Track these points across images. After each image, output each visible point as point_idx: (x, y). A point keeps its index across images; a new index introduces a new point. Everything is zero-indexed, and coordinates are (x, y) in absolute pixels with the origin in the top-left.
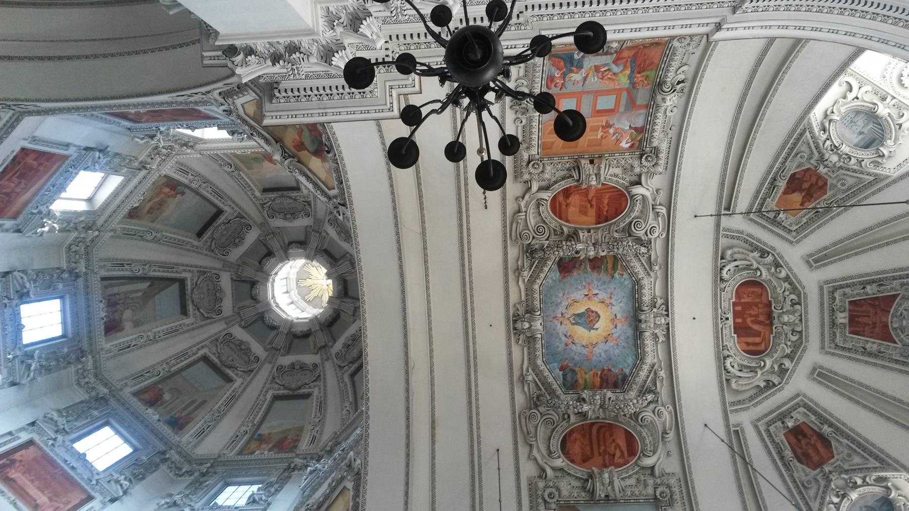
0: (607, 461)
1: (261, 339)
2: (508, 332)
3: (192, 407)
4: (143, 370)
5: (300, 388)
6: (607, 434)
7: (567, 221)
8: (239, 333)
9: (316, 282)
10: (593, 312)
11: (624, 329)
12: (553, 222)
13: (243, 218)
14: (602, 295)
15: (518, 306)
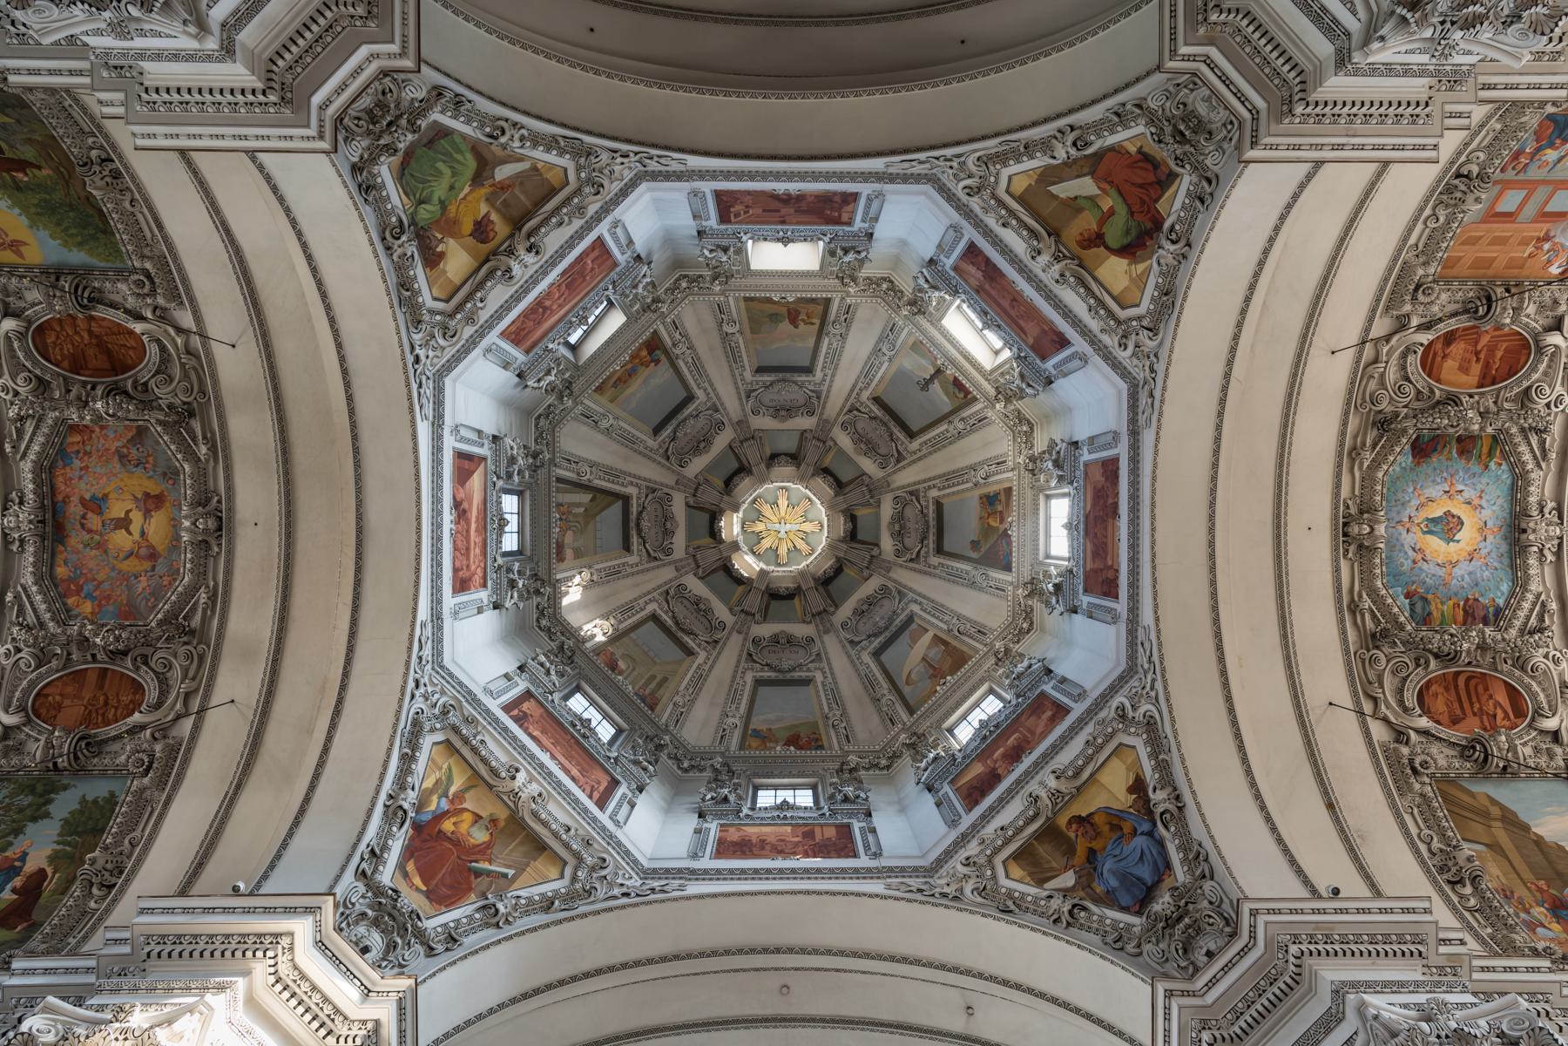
0: (1487, 724)
1: (724, 598)
2: (1335, 538)
3: (652, 686)
5: (793, 669)
6: (1481, 689)
7: (1438, 381)
8: (696, 587)
9: (770, 526)
10: (1453, 516)
11: (1494, 544)
12: (1420, 379)
13: (717, 410)
14: (1469, 493)
15: (1350, 502)
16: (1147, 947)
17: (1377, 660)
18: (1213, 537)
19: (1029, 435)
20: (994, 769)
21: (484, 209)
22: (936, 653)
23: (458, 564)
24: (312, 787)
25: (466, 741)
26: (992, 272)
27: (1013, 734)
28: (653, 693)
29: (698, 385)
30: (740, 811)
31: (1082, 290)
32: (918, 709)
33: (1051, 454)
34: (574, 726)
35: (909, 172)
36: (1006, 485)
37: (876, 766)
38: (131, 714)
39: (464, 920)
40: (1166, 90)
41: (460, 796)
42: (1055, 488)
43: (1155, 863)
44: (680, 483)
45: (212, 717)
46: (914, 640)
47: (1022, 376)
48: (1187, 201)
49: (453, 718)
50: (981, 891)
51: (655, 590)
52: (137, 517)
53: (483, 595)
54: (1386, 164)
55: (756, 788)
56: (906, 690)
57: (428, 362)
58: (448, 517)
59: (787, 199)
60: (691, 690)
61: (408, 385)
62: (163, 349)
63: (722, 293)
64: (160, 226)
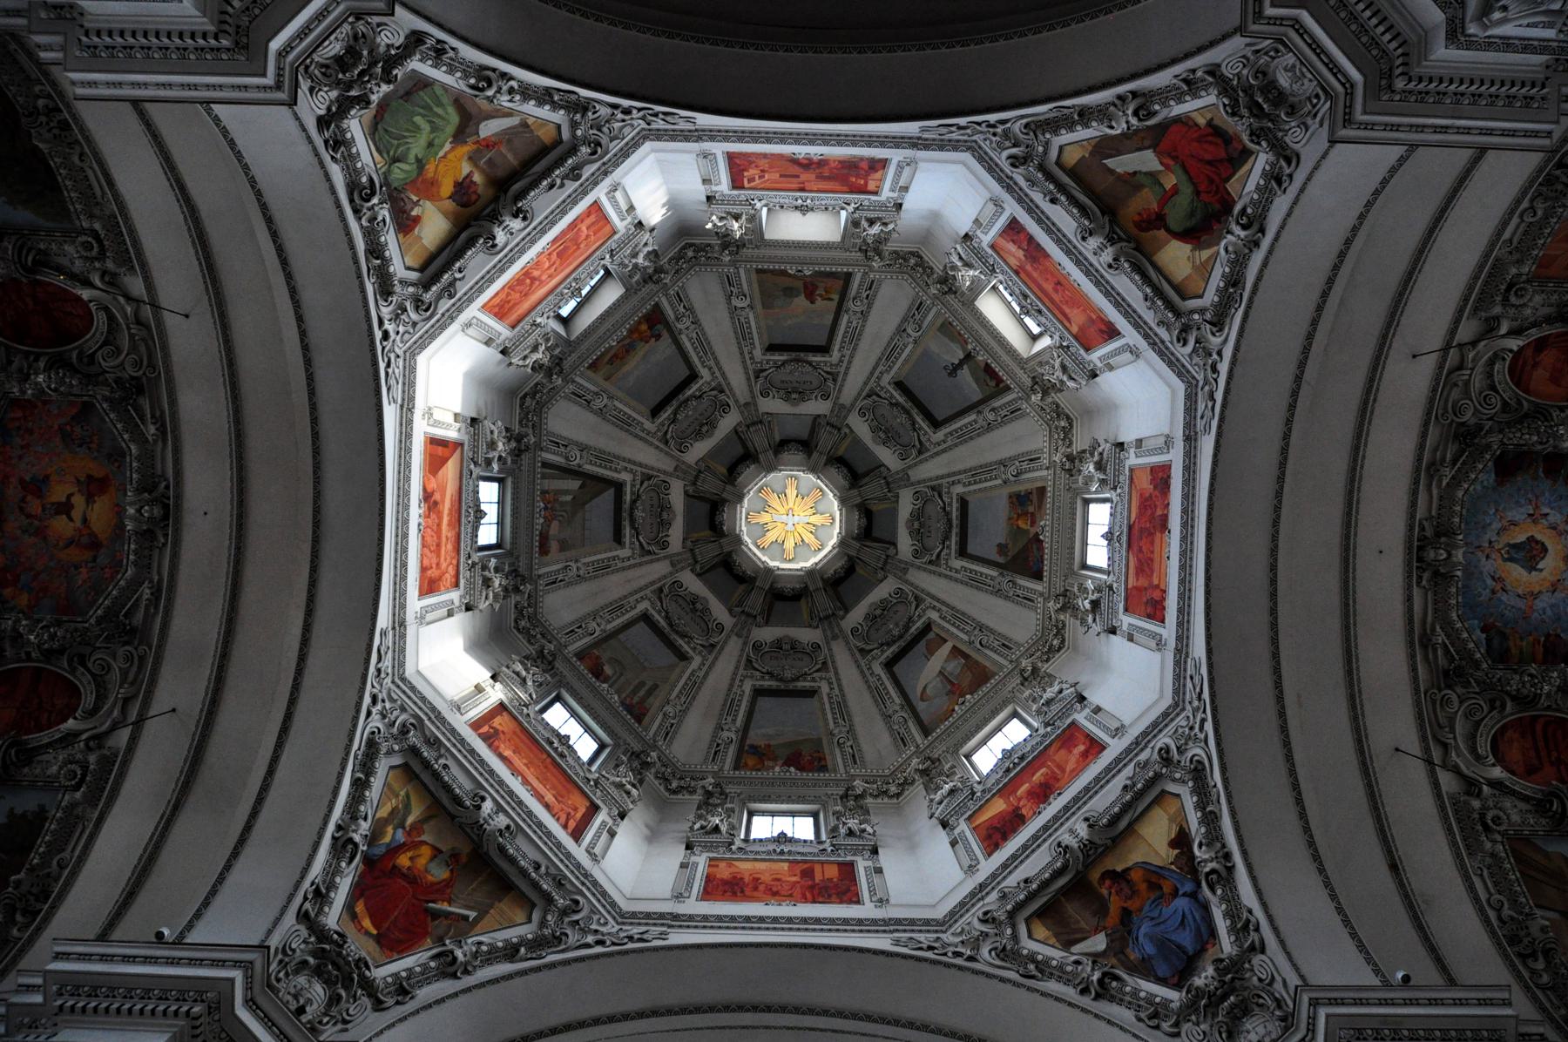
2: (1408, 563)
3: (642, 693)
4: (572, 623)
5: (797, 679)
7: (1527, 391)
8: (692, 583)
9: (776, 517)
10: (1537, 542)
13: (722, 391)
16: (1186, 1027)
17: (1449, 702)
18: (1276, 560)
19: (1067, 432)
20: (1018, 808)
21: (466, 168)
22: (954, 666)
23: (426, 562)
24: (254, 813)
25: (426, 765)
26: (1034, 251)
27: (1040, 768)
28: (643, 700)
29: (702, 363)
30: (732, 843)
31: (1137, 278)
32: (934, 730)
33: (1092, 455)
34: (551, 743)
35: (946, 137)
36: (1039, 484)
37: (885, 793)
38: (65, 720)
39: (418, 969)
40: (1244, 57)
41: (417, 828)
42: (1096, 492)
43: (1198, 929)
44: (680, 470)
45: (151, 727)
46: (931, 651)
47: (1064, 368)
48: (1262, 182)
49: (413, 738)
50: (1002, 953)
51: (647, 586)
52: (79, 501)
53: (455, 596)
54: (1482, 151)
55: (751, 814)
56: (921, 707)
57: (398, 338)
58: (416, 511)
59: (808, 164)
60: (683, 699)
61: (375, 364)
62: (111, 318)
63: (733, 263)
64: (111, 183)
